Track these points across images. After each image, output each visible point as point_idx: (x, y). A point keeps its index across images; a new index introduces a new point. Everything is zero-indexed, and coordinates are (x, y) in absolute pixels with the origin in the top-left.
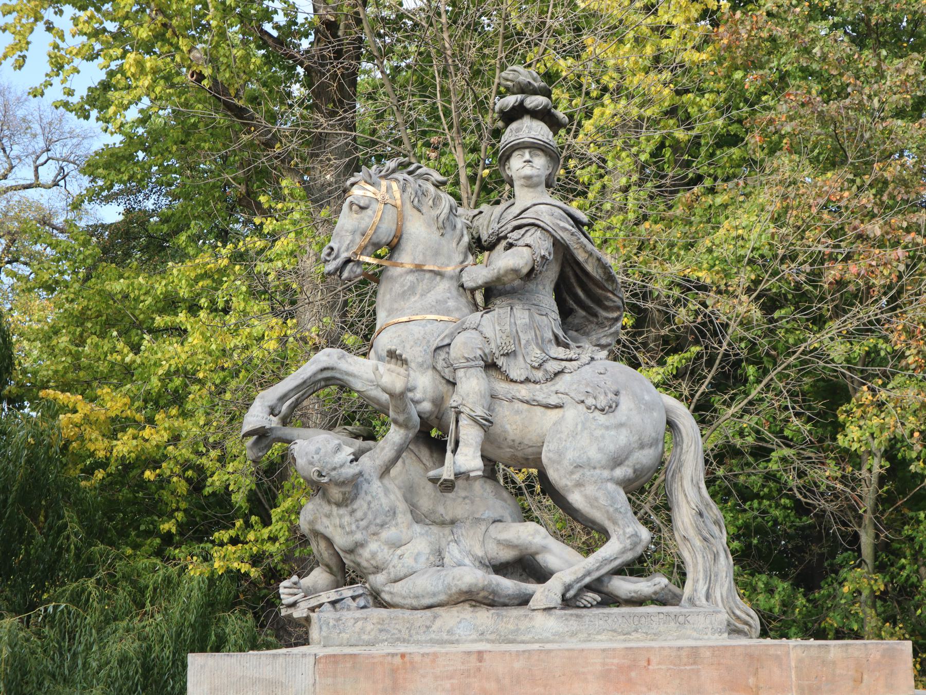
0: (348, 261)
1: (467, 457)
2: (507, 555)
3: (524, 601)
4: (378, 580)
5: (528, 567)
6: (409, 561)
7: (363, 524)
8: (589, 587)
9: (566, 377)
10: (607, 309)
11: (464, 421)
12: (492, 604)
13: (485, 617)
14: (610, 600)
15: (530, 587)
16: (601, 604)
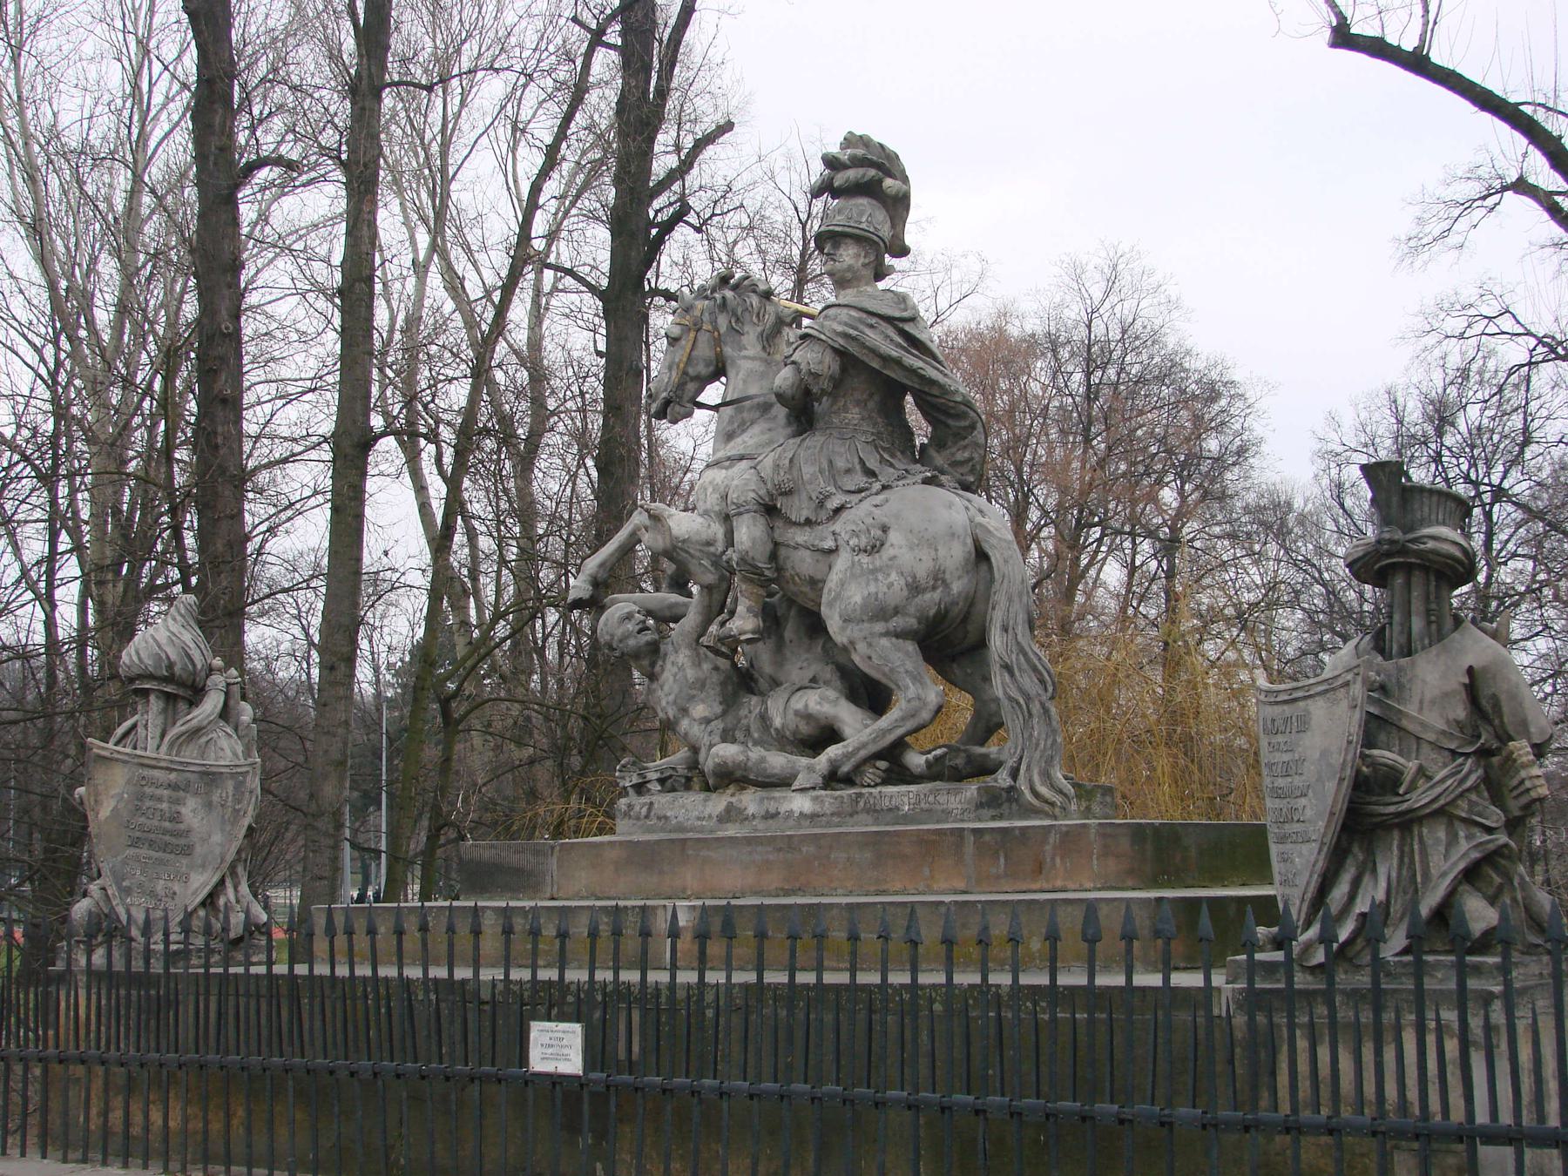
2: (805, 729)
7: (671, 698)
9: (845, 515)
14: (898, 774)
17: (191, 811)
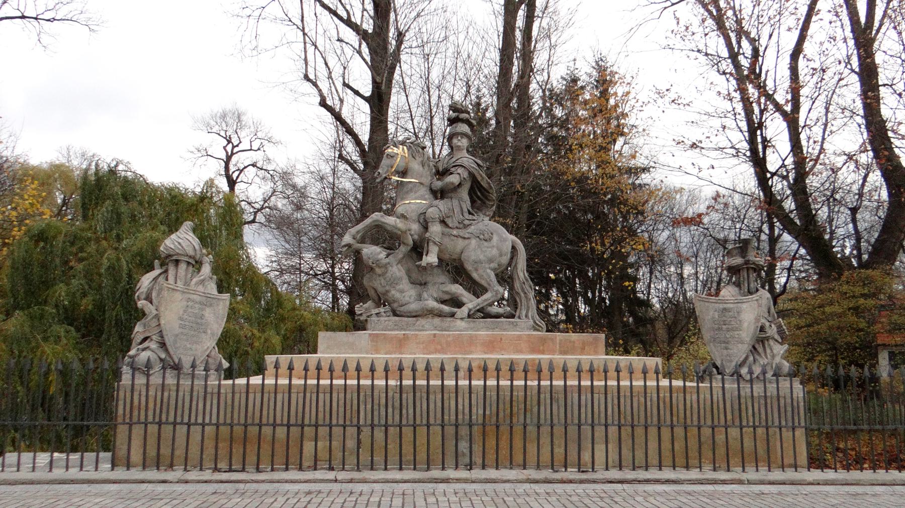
0: (386, 178)
1: (431, 258)
2: (447, 297)
3: (453, 315)
4: (395, 305)
6: (407, 299)
8: (478, 311)
9: (473, 227)
10: (489, 200)
11: (431, 244)
12: (440, 316)
13: (437, 321)
14: (488, 316)
15: (455, 310)
16: (483, 318)
17: (208, 314)
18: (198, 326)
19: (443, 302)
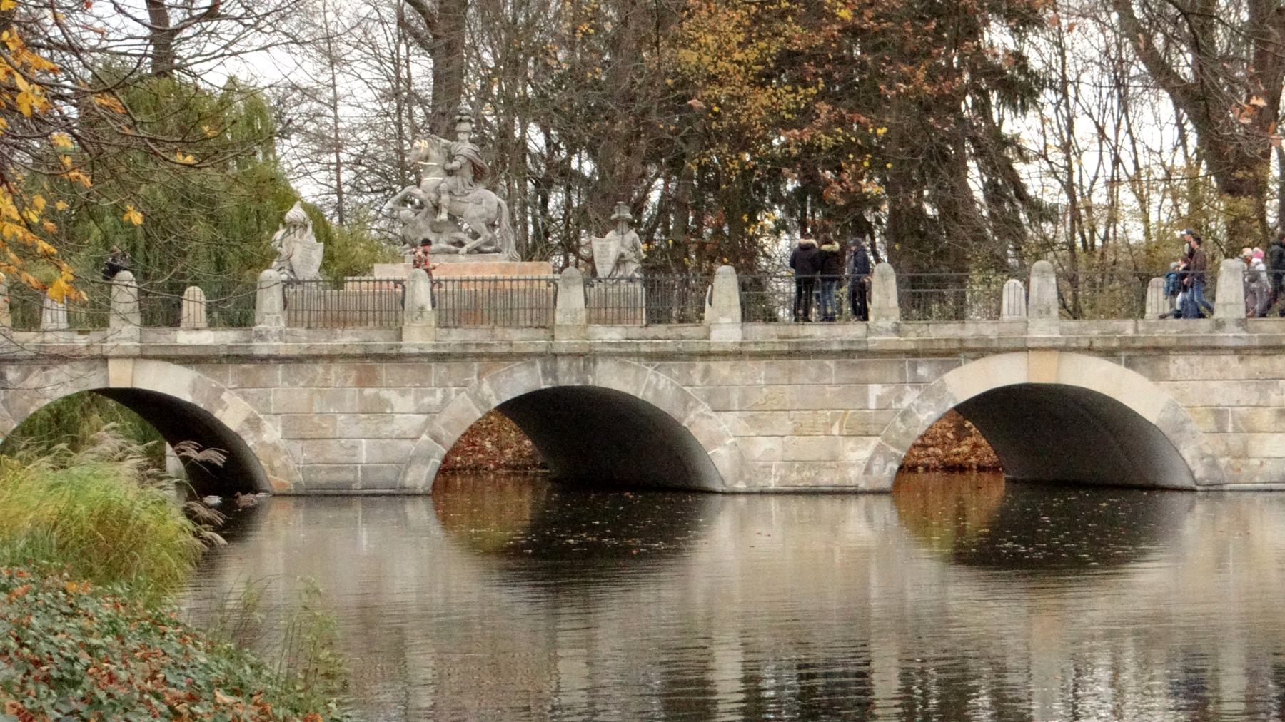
1: (444, 216)
3: (457, 252)
5: (461, 244)
18: (308, 261)
19: (453, 244)
